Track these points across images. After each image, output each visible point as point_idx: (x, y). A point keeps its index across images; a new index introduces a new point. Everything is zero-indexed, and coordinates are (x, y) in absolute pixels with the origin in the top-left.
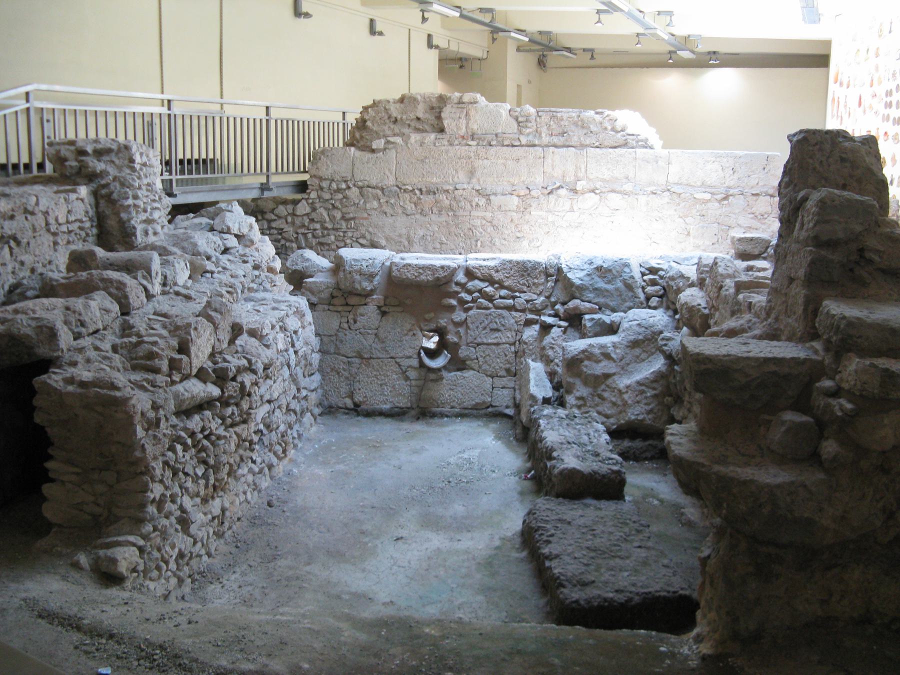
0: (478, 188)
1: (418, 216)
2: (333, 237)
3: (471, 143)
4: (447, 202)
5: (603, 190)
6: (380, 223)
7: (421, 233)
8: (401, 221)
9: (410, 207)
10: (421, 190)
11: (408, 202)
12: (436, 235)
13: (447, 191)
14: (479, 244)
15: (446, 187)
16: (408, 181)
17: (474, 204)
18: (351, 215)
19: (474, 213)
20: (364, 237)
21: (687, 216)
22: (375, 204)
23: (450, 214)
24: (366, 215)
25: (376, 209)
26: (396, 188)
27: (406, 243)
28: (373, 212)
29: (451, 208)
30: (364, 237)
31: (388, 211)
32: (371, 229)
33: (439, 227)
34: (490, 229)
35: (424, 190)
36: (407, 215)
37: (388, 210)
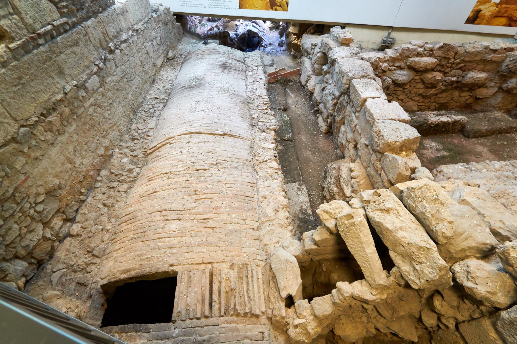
0: (75, 83)
1: (60, 138)
2: (16, 226)
3: (41, 41)
4: (67, 110)
5: (119, 44)
6: (41, 170)
7: (71, 149)
8: (54, 152)
9: (49, 136)
10: (42, 114)
11: (45, 133)
12: (80, 140)
13: (61, 100)
14: (101, 124)
15: (59, 97)
16: (28, 114)
17: (81, 98)
18: (11, 191)
19: (87, 105)
20: (38, 194)
21: (144, 43)
22: (22, 160)
23: (75, 117)
24: (23, 177)
25: (27, 163)
26: (22, 130)
27: (69, 166)
28: (27, 167)
29: (72, 112)
30: (38, 194)
31: (38, 154)
32: (39, 183)
33: (77, 134)
34: (99, 110)
35: (45, 112)
36: (52, 144)
37: (38, 154)
